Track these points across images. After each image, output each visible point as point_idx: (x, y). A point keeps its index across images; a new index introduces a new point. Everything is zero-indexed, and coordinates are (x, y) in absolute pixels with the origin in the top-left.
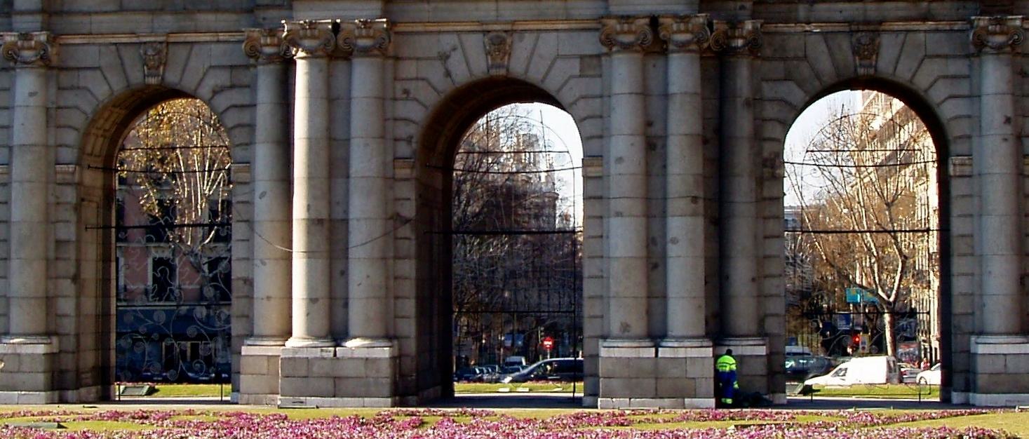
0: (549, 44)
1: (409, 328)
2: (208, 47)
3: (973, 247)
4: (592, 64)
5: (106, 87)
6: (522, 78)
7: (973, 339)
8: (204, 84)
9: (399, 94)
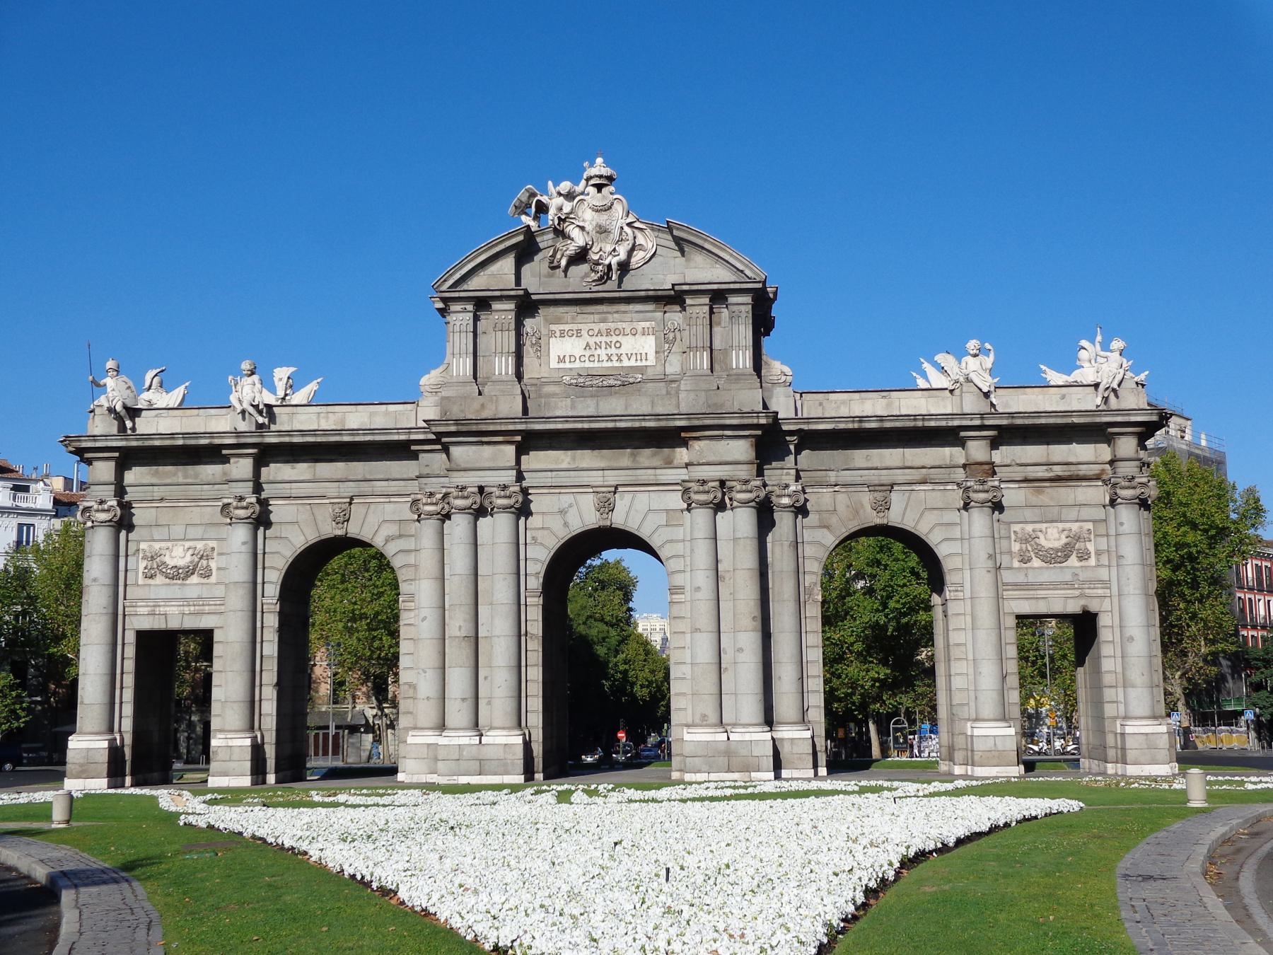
0: (644, 500)
1: (535, 720)
2: (381, 506)
5: (302, 538)
6: (623, 528)
7: (969, 724)
8: (378, 534)
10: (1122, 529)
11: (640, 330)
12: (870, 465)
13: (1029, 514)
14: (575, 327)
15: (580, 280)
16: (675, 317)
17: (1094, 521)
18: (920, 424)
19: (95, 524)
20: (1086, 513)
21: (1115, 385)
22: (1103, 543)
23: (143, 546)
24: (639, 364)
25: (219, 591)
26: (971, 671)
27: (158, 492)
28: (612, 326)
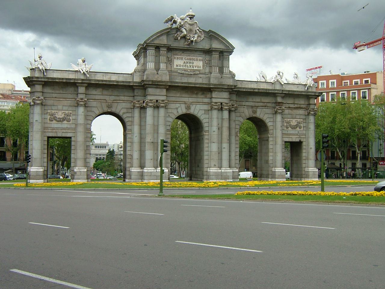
0: (199, 107)
2: (122, 103)
3: (273, 151)
4: (207, 111)
7: (273, 168)
9: (167, 116)
10: (310, 121)
11: (199, 59)
12: (253, 101)
13: (289, 116)
14: (181, 57)
15: (182, 44)
16: (207, 57)
17: (303, 119)
18: (268, 91)
19: (35, 104)
20: (302, 117)
21: (311, 85)
22: (305, 125)
23: (49, 111)
24: (198, 69)
25: (73, 126)
26: (274, 155)
27: (54, 95)
28: (191, 57)
